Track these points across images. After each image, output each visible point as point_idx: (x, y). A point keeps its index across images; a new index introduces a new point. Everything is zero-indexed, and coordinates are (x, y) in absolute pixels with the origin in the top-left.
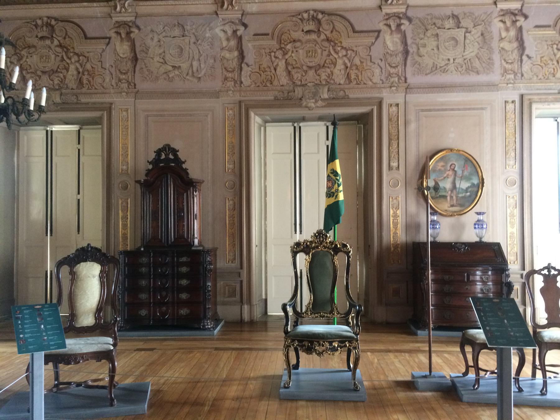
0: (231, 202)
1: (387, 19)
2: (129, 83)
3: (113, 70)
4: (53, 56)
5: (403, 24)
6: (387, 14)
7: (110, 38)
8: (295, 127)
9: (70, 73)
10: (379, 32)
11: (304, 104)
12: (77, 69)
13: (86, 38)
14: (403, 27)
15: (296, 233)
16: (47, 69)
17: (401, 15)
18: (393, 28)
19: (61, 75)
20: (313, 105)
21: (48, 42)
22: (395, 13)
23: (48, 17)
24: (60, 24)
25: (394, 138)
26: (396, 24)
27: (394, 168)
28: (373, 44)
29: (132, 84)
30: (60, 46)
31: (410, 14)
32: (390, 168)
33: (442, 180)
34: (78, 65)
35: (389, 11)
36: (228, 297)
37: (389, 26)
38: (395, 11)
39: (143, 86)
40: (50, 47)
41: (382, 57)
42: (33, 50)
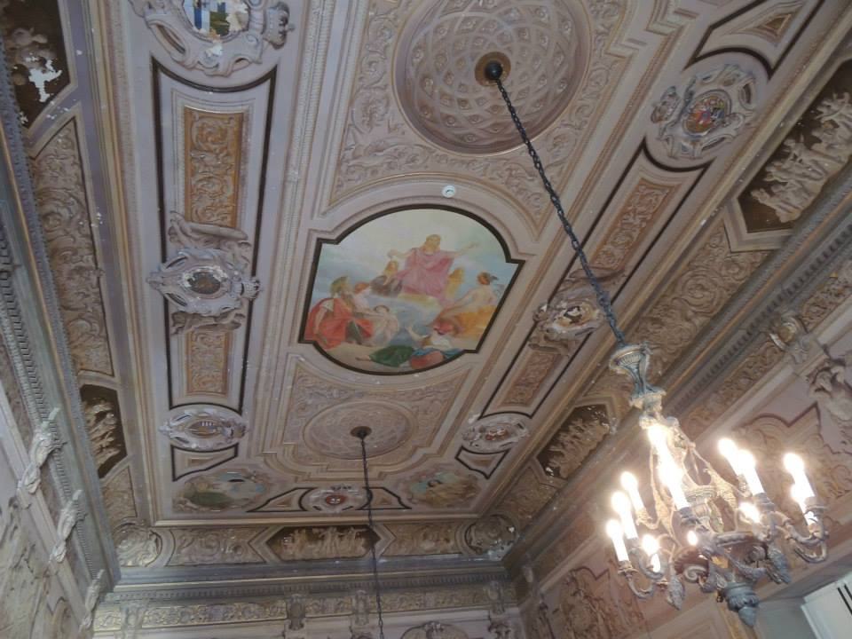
1: (814, 383)
5: (836, 374)
6: (809, 376)
7: (607, 570)
8: (839, 589)
10: (815, 405)
12: (602, 617)
13: (596, 579)
14: (839, 379)
16: (587, 626)
17: (827, 365)
18: (828, 387)
19: (595, 628)
21: (578, 597)
22: (817, 368)
23: (571, 571)
24: (579, 573)
26: (828, 381)
28: (819, 426)
30: (586, 597)
31: (835, 354)
35: (808, 371)
37: (822, 389)
38: (815, 365)
41: (843, 439)
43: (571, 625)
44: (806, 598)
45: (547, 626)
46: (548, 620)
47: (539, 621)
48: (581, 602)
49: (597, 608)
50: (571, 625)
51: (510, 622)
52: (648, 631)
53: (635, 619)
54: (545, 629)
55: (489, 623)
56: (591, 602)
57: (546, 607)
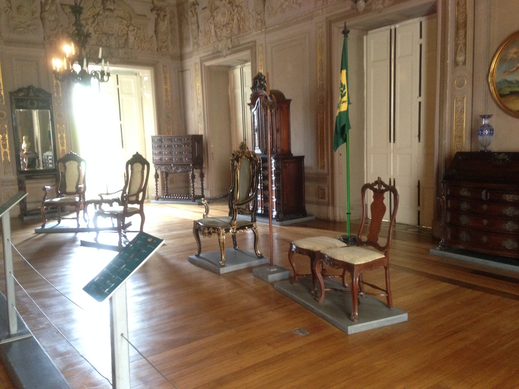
0: (322, 115)
2: (262, 21)
3: (253, 13)
4: (227, 12)
9: (235, 22)
11: (373, 8)
12: (237, 18)
15: (390, 142)
19: (231, 25)
20: (381, 6)
25: (461, 26)
27: (461, 63)
29: (263, 23)
32: (456, 64)
33: (514, 71)
34: (238, 15)
36: (322, 198)
39: (269, 21)
40: (225, 5)
42: (218, 10)
43: (213, 20)
44: (370, 32)
45: (195, 18)
46: (197, 15)
47: (190, 13)
48: (225, 5)
49: (235, 12)
50: (213, 20)
51: (168, 10)
52: (266, 33)
53: (260, 24)
54: (194, 19)
55: (152, 6)
56: (232, 7)
57: (198, 4)
